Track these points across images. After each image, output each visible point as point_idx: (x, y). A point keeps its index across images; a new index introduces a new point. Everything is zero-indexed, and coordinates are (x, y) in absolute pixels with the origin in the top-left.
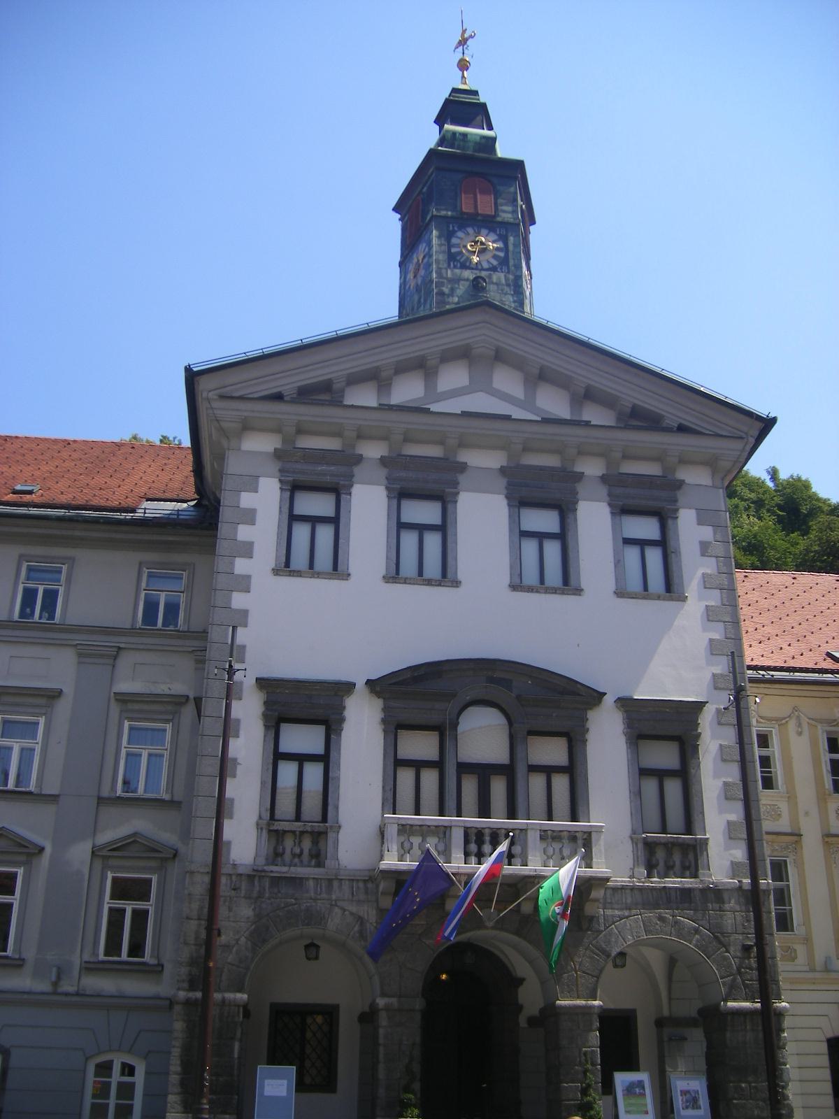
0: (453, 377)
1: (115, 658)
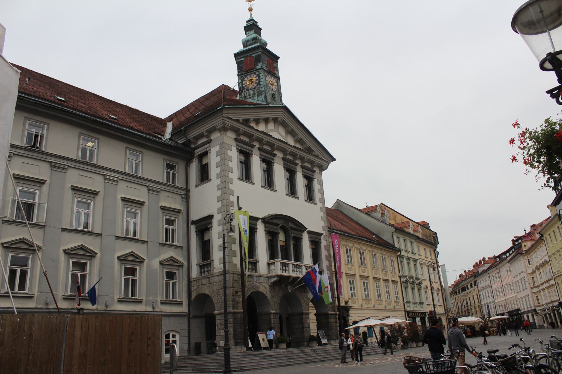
0: (271, 126)
1: (159, 192)
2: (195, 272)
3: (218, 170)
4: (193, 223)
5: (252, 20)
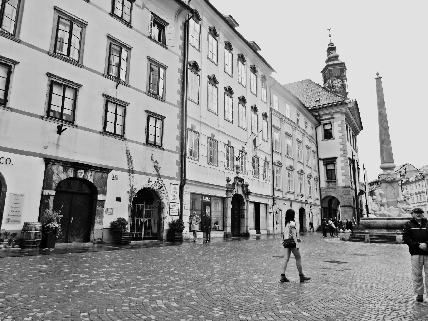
2: (323, 184)
3: (341, 134)
4: (320, 159)
5: (333, 44)
